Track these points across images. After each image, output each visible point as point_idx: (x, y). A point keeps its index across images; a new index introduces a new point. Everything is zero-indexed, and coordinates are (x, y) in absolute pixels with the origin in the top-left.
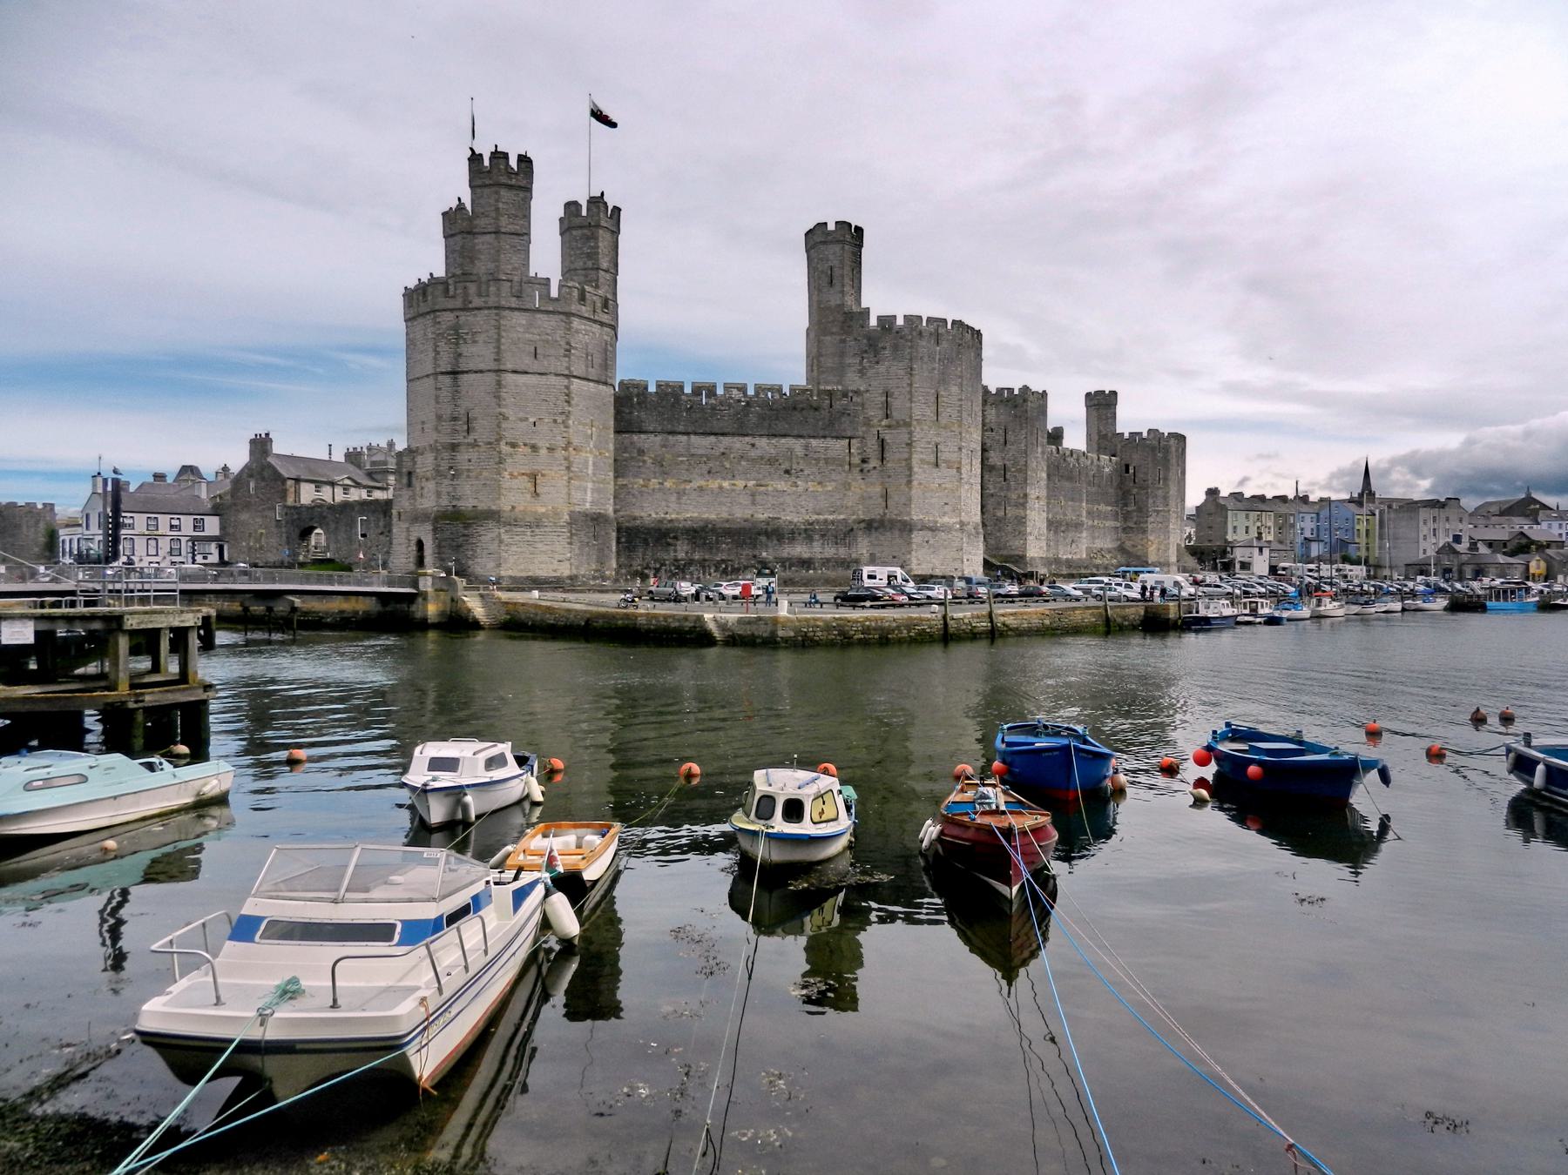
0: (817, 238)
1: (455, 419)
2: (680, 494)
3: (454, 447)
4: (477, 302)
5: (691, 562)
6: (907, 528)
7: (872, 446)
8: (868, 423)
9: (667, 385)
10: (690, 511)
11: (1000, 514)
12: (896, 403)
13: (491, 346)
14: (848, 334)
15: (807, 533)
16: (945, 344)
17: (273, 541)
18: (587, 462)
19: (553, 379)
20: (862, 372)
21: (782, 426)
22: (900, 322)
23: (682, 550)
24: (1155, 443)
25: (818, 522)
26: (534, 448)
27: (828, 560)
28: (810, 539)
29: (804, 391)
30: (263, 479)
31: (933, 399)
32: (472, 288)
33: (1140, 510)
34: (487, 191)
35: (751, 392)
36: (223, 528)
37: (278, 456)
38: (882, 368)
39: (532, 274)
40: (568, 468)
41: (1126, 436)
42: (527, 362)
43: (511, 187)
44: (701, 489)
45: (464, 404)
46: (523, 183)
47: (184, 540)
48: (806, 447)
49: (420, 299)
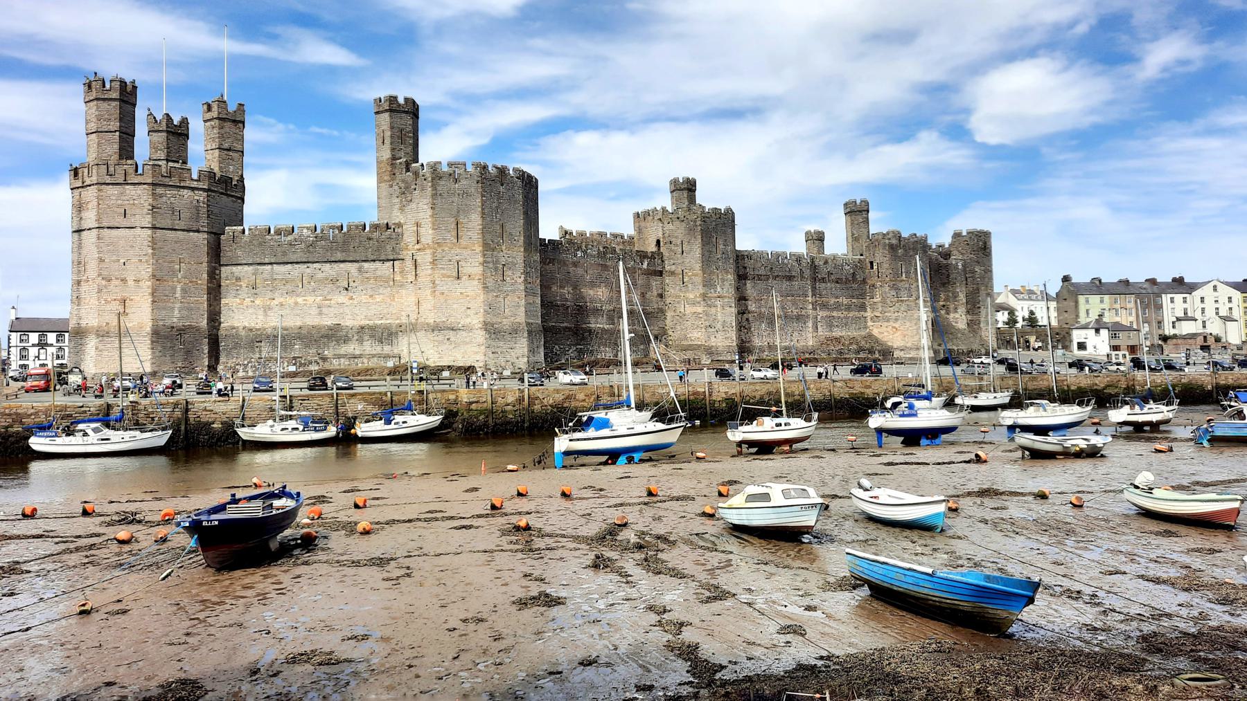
2: (267, 309)
7: (409, 264)
12: (422, 231)
18: (174, 289)
19: (138, 231)
20: (402, 209)
28: (361, 341)
31: (454, 226)
45: (84, 252)
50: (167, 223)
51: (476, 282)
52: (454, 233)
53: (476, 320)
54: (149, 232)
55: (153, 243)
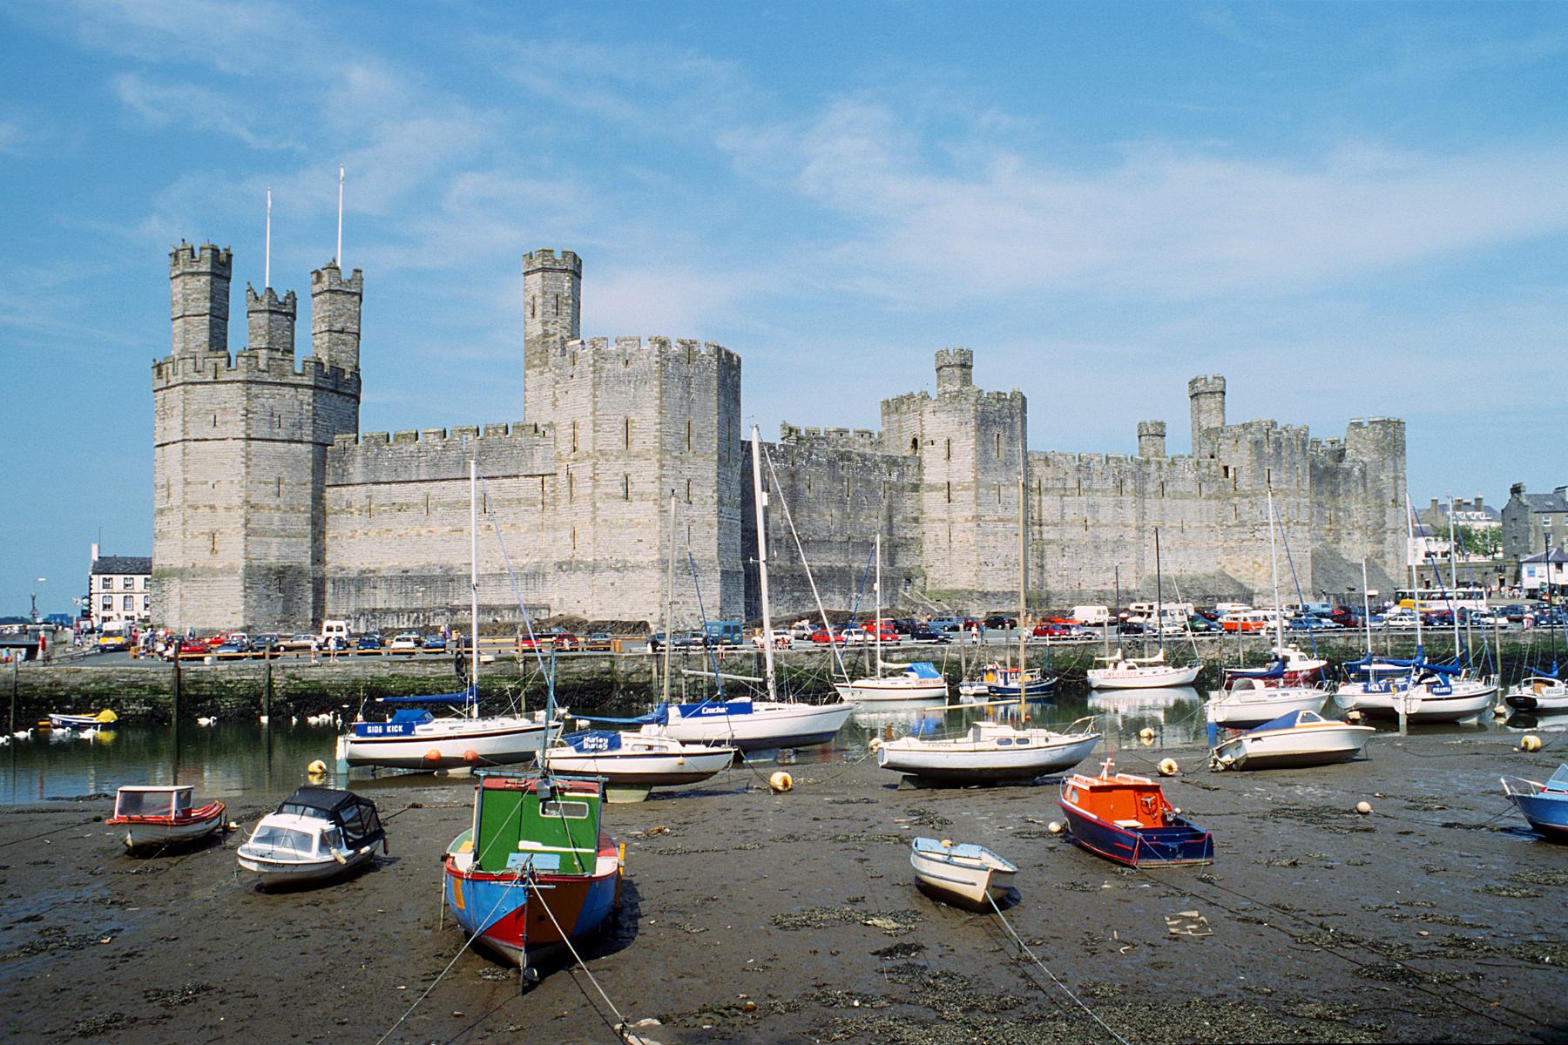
3: (161, 511)
8: (559, 458)
12: (580, 434)
26: (212, 507)
31: (622, 426)
43: (193, 274)
48: (499, 488)
50: (264, 431)
54: (242, 444)
55: (247, 457)
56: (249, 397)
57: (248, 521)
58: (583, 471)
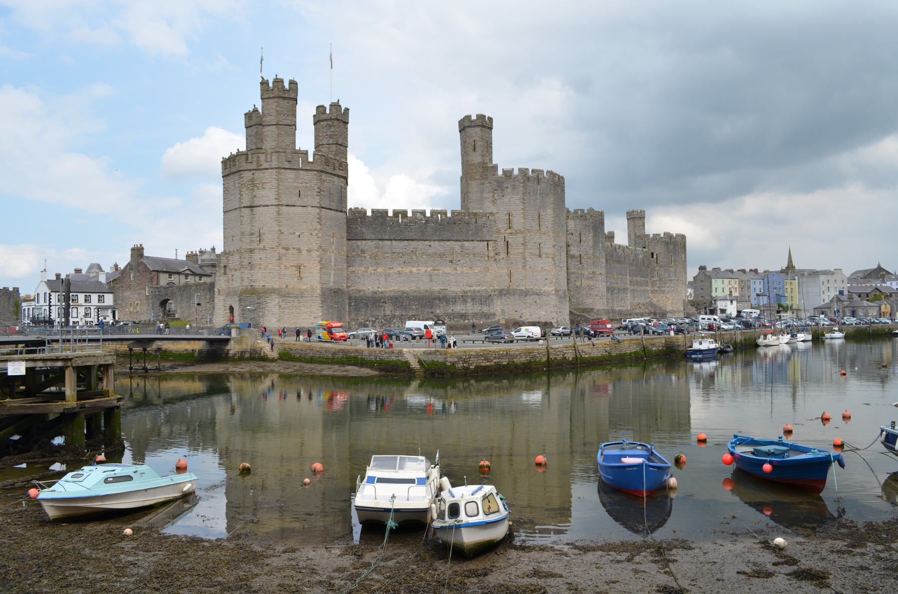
0: (465, 125)
1: (252, 234)
2: (387, 276)
3: (251, 251)
4: (265, 165)
5: (394, 317)
6: (526, 293)
7: (501, 245)
8: (498, 231)
9: (378, 211)
10: (392, 287)
11: (578, 284)
12: (514, 220)
13: (274, 192)
14: (486, 179)
15: (464, 298)
16: (543, 185)
17: (145, 308)
18: (331, 258)
19: (310, 209)
20: (494, 202)
21: (447, 235)
22: (516, 172)
23: (388, 310)
24: (668, 240)
25: (470, 291)
27: (477, 314)
29: (459, 214)
30: (139, 271)
31: (537, 217)
32: (262, 157)
33: (661, 280)
34: (271, 101)
35: (428, 214)
36: (115, 301)
37: (147, 257)
38: (506, 199)
39: (297, 148)
40: (320, 262)
41: (651, 236)
42: (295, 200)
43: (284, 98)
44: (399, 272)
46: (292, 95)
47: (92, 308)
48: (462, 247)
49: (232, 166)
51: (550, 260)
52: (537, 222)
53: (550, 288)
54: (318, 211)
56: (322, 181)
57: (321, 259)
58: (516, 241)
